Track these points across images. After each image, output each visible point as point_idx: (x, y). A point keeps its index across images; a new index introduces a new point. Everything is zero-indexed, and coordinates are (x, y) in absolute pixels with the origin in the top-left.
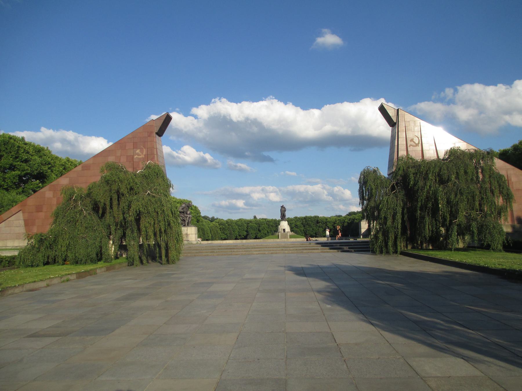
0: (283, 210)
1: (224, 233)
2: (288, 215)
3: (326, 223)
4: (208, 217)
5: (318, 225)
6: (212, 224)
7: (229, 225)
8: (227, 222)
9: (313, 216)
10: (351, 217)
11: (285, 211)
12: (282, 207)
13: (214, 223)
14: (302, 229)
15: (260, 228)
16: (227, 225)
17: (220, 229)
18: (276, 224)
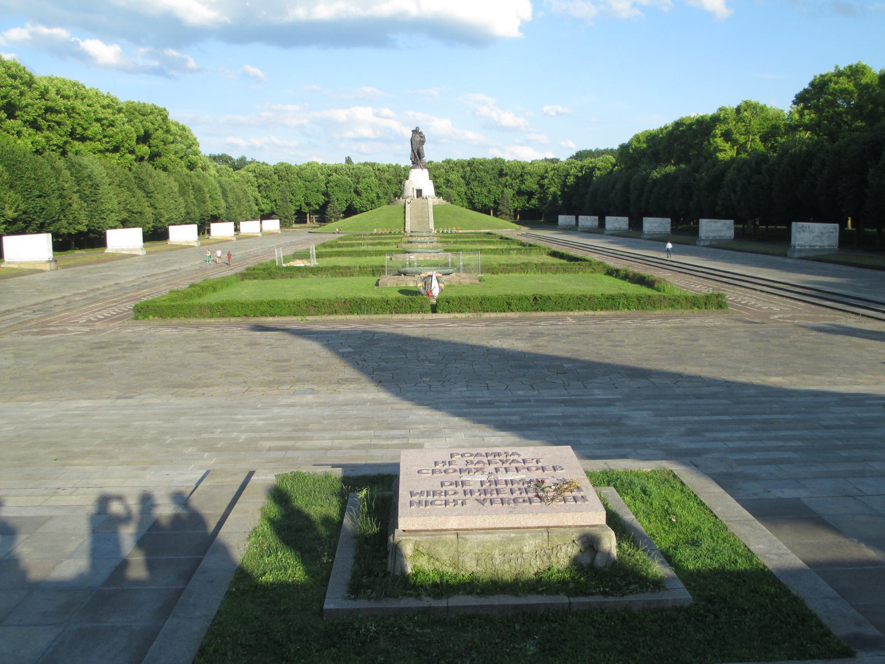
1: (267, 197)
2: (433, 154)
3: (522, 176)
4: (231, 159)
5: (503, 180)
6: (236, 176)
7: (280, 178)
8: (276, 171)
10: (586, 162)
12: (416, 132)
13: (242, 172)
14: (463, 189)
15: (360, 187)
16: (275, 177)
17: (259, 187)
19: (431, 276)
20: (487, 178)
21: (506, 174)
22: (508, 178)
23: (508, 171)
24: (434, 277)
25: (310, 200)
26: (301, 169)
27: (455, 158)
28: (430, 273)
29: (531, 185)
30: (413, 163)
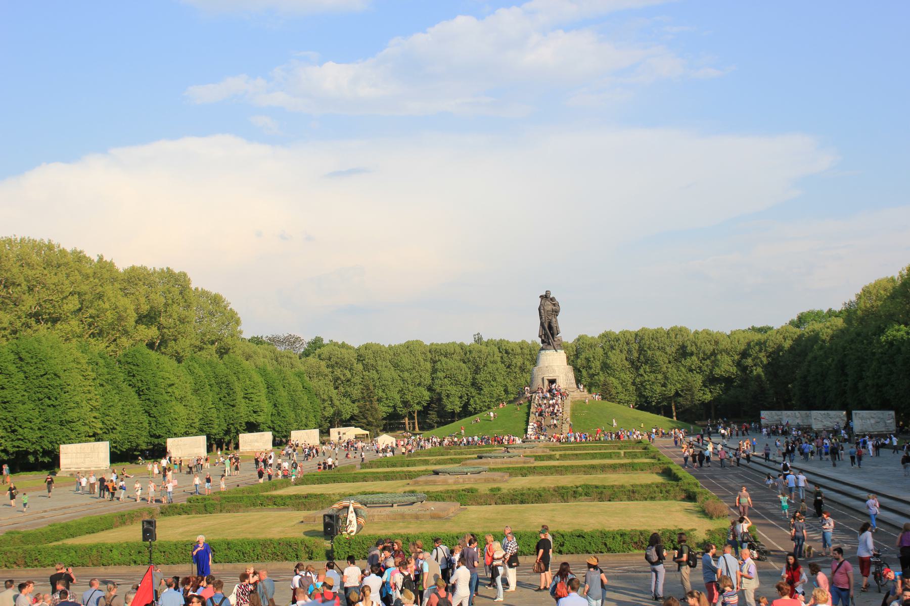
0: (549, 307)
3: (714, 353)
5: (688, 362)
7: (366, 368)
9: (667, 327)
11: (556, 312)
12: (545, 297)
14: (628, 377)
15: (480, 378)
18: (516, 361)
19: (347, 508)
20: (661, 359)
21: (692, 354)
22: (694, 358)
23: (694, 348)
24: (351, 509)
25: (409, 397)
26: (395, 352)
27: (617, 329)
28: (345, 503)
29: (727, 368)
30: (543, 342)
